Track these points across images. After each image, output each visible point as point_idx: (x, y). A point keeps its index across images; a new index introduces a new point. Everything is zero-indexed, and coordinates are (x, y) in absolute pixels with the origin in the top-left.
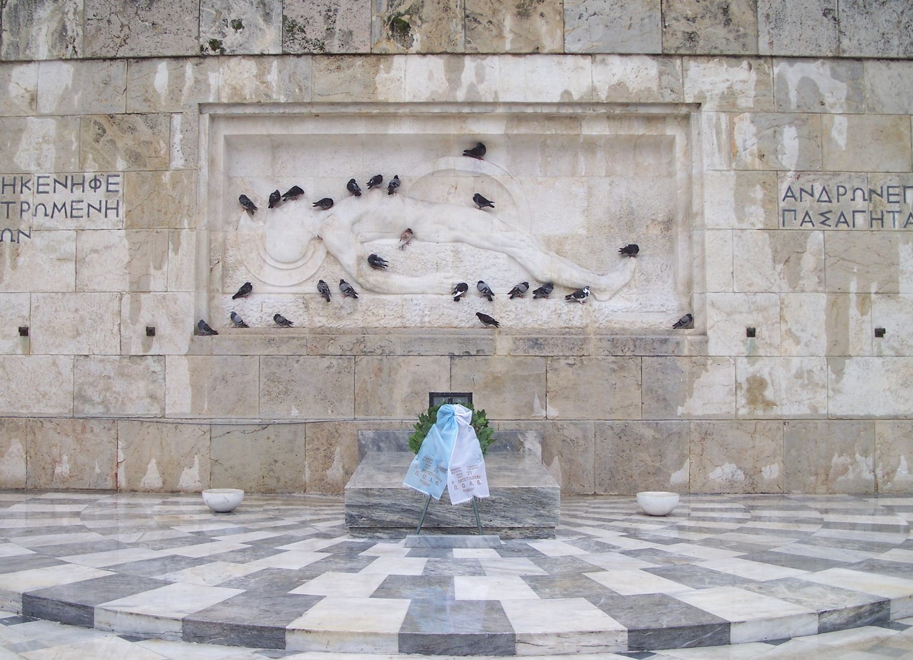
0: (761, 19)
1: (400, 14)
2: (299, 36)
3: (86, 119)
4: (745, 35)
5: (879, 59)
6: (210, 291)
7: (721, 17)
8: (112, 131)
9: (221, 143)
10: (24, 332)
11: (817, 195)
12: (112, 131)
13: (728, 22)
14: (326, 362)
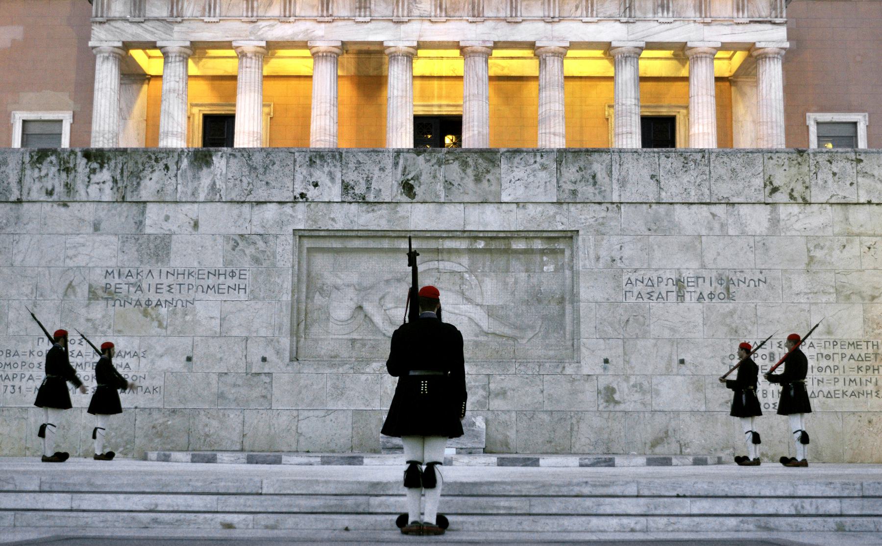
0: (614, 181)
1: (408, 180)
2: (351, 191)
3: (227, 238)
4: (605, 191)
5: (683, 203)
6: (297, 337)
7: (591, 180)
8: (242, 244)
9: (305, 251)
10: (189, 359)
11: (645, 282)
12: (242, 244)
13: (595, 183)
14: (363, 377)
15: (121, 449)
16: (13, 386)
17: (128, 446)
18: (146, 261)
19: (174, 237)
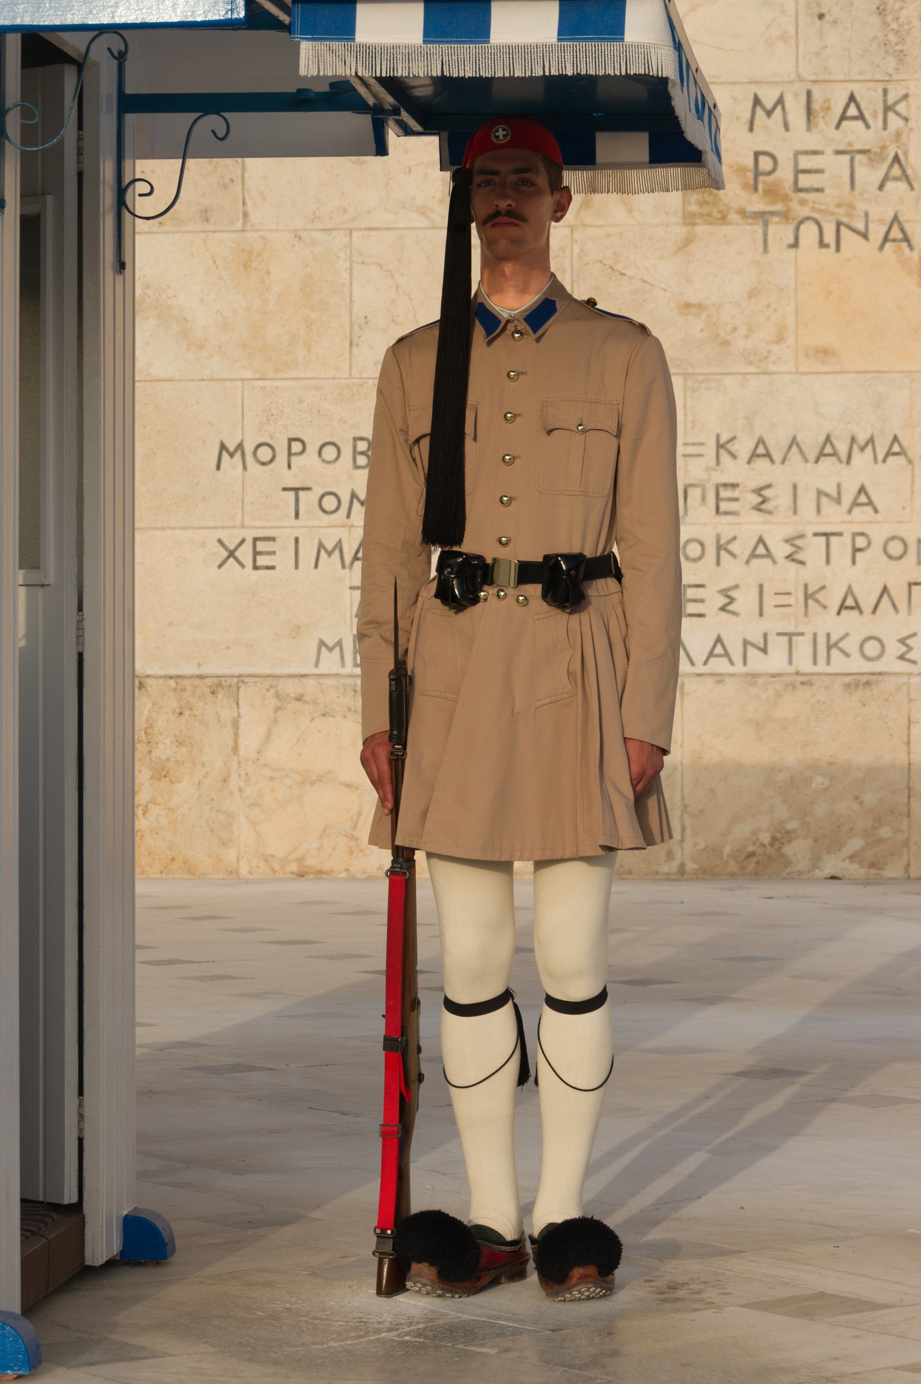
15: (855, 844)
17: (885, 832)
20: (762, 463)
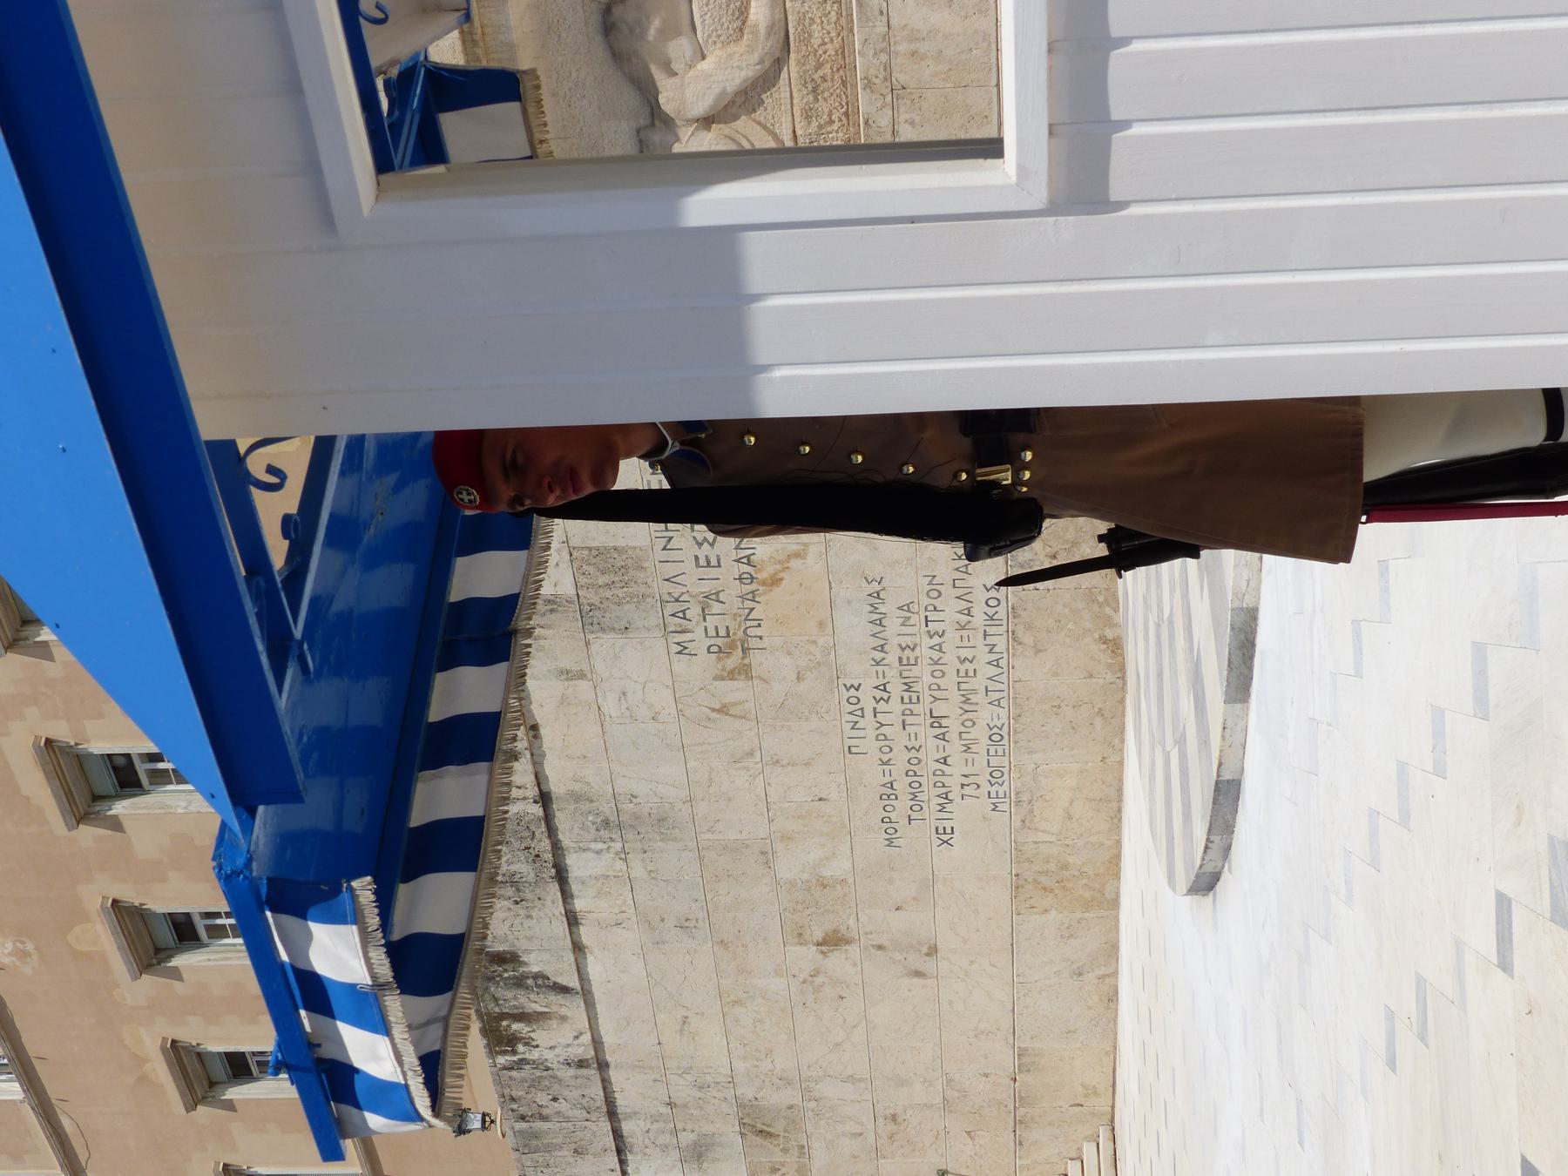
16: (963, 785)
17: (1101, 599)
18: (643, 589)
19: (574, 542)
20: (886, 648)
